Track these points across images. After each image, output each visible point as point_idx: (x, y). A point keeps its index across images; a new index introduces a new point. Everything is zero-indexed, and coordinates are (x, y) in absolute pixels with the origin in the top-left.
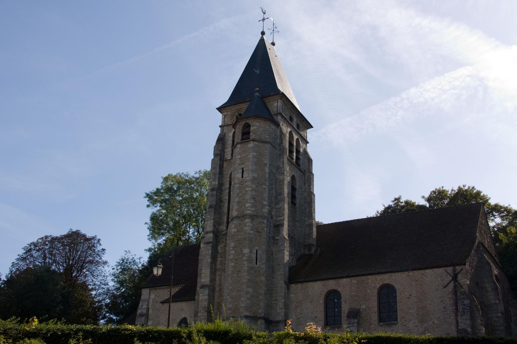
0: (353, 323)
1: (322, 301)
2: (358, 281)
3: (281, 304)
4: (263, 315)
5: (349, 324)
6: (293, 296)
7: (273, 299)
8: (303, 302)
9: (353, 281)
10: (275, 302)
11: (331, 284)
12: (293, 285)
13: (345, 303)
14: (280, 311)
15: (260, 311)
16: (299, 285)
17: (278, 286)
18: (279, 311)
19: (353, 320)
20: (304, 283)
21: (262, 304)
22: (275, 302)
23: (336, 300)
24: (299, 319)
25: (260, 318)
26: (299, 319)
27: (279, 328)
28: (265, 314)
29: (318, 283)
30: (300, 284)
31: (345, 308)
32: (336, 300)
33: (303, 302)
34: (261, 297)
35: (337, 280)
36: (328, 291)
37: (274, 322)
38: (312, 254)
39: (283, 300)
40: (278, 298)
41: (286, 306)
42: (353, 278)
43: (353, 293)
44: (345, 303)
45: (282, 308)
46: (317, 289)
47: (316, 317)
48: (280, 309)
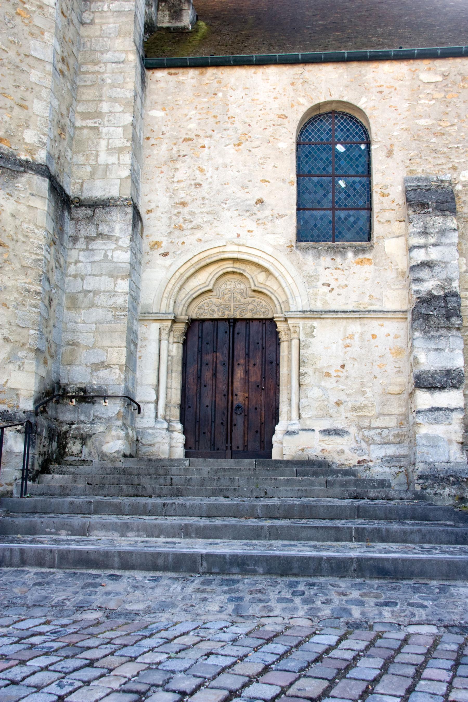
0: (443, 232)
1: (287, 143)
2: (445, 76)
3: (115, 131)
4: (41, 156)
5: (425, 233)
6: (157, 113)
7: (80, 108)
8: (206, 142)
9: (425, 77)
10: (90, 123)
11: (329, 83)
12: (160, 74)
13: (390, 154)
14: (113, 159)
15: (30, 136)
16: (190, 76)
17: (108, 56)
18: (103, 158)
19: (439, 220)
20: (211, 71)
21: (40, 108)
22: (90, 123)
23: (340, 148)
24: (184, 204)
25: (27, 166)
26: (184, 204)
27: (104, 229)
28: (50, 156)
29: (272, 71)
30: (192, 73)
31: (388, 178)
32: (340, 148)
33: (206, 142)
34: (35, 76)
35: (355, 67)
36: (318, 106)
37: (81, 204)
38: (184, 28)
39: (128, 118)
40: (105, 107)
41: (137, 144)
42: (424, 64)
43: (422, 122)
44: (390, 154)
45: (120, 150)
46: (269, 100)
47: (260, 201)
48: (110, 150)
